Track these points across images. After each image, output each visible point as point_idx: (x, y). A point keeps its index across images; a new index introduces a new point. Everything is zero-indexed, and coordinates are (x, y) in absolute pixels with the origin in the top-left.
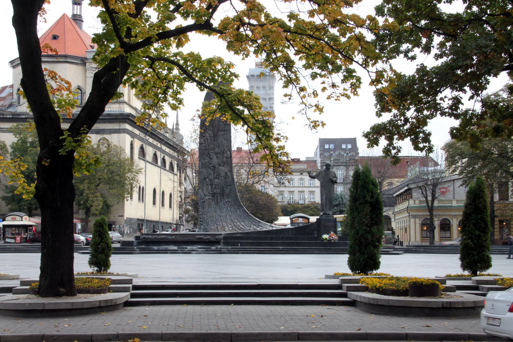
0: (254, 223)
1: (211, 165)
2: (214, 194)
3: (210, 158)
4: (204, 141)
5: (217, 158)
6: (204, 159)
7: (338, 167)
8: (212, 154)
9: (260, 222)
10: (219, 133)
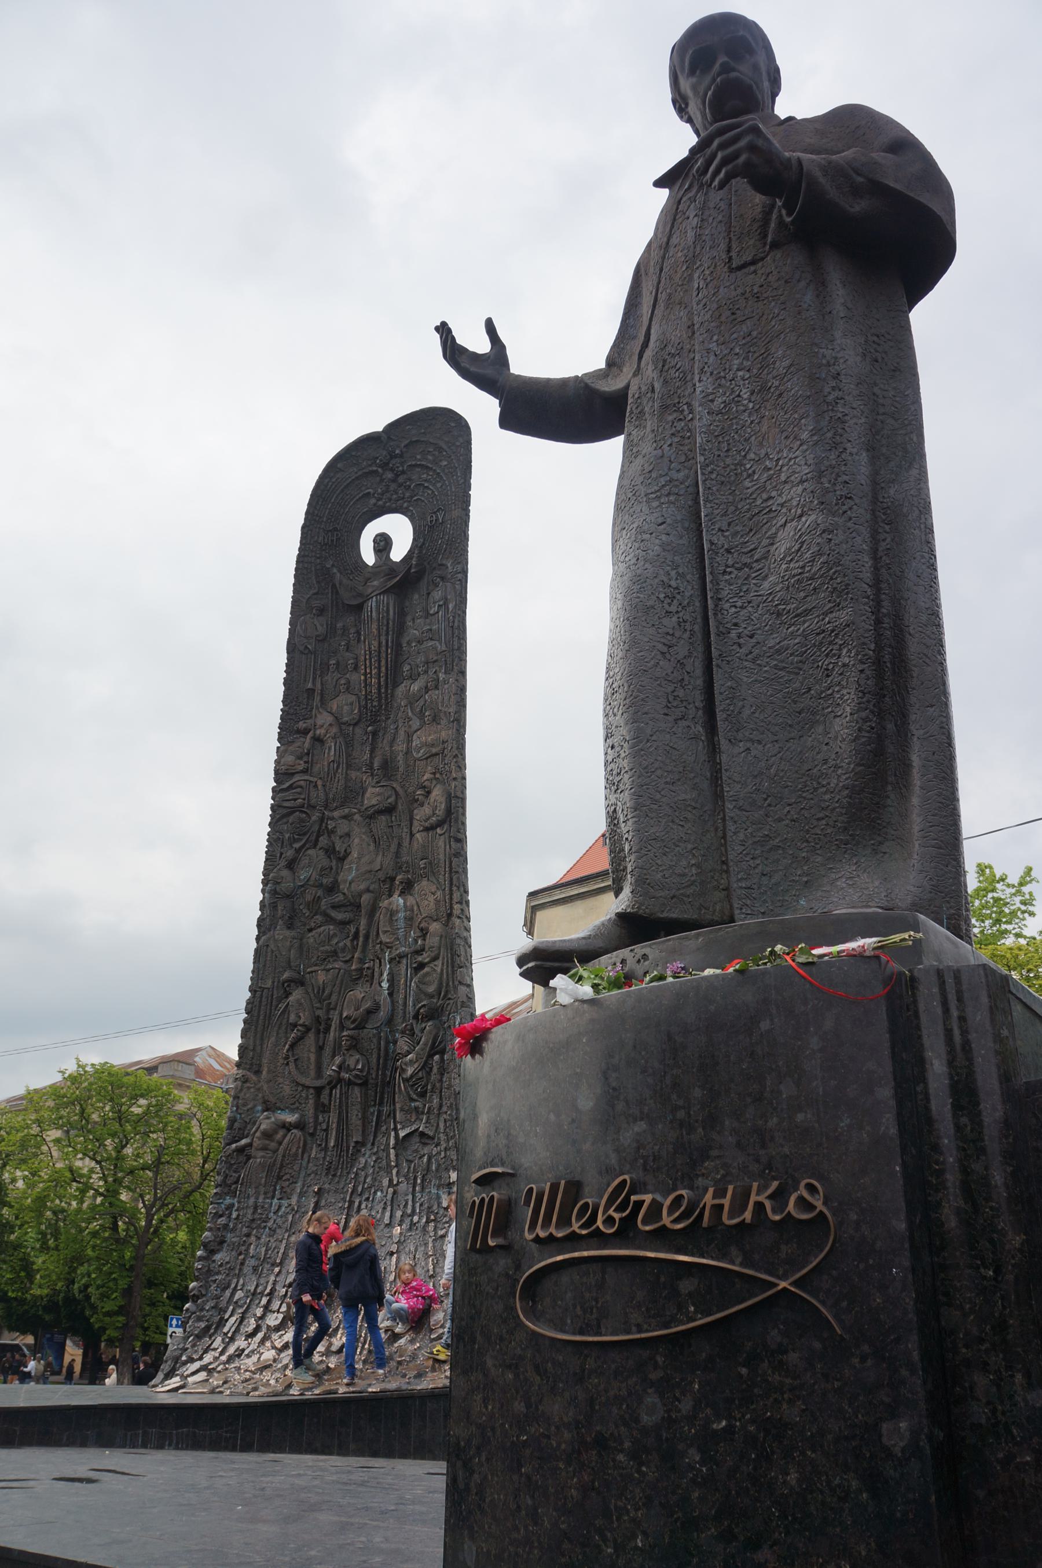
3: (330, 851)
6: (291, 865)
8: (343, 827)
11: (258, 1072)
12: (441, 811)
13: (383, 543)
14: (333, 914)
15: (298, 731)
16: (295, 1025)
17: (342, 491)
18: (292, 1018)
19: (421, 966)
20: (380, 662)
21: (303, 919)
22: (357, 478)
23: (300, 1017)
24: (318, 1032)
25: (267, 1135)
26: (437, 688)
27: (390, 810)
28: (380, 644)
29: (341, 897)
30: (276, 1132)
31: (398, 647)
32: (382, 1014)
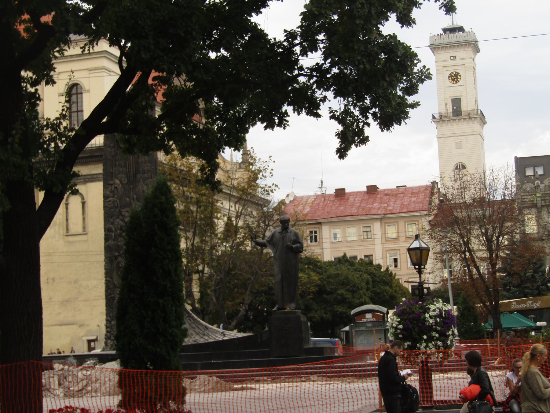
0: (197, 330)
4: (112, 192)
6: (112, 224)
9: (207, 328)
11: (112, 278)
15: (110, 184)
26: (151, 178)
31: (138, 163)
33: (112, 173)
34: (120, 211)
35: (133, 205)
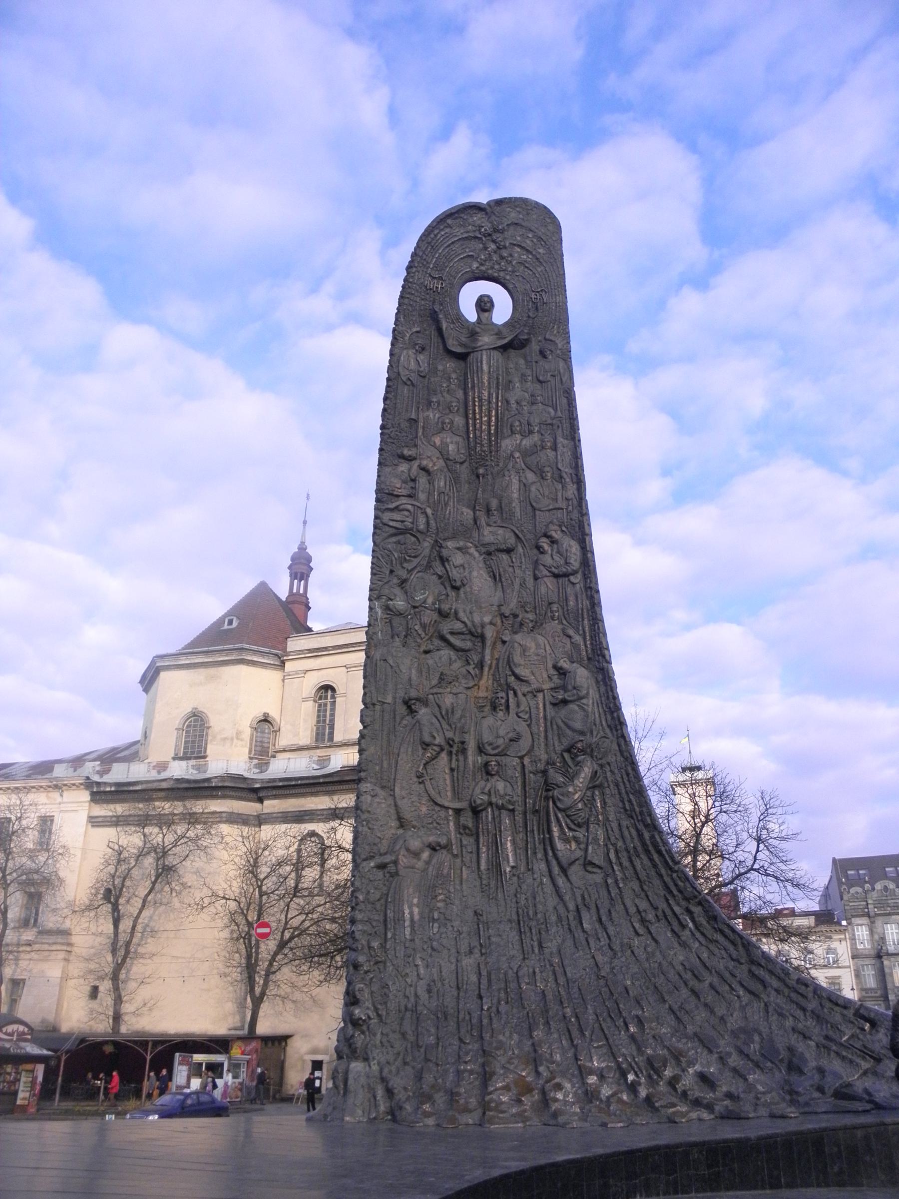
1: (446, 627)
2: (476, 812)
5: (496, 577)
7: (886, 918)
10: (507, 444)
12: (575, 563)
13: (484, 305)
14: (452, 639)
15: (402, 457)
16: (426, 745)
17: (449, 246)
18: (427, 739)
19: (565, 702)
20: (490, 411)
21: (419, 640)
22: (463, 239)
23: (434, 738)
24: (450, 753)
25: (416, 855)
27: (509, 551)
28: (490, 395)
29: (458, 626)
30: (422, 851)
32: (525, 744)
33: (416, 421)
34: (438, 545)
35: (486, 531)
